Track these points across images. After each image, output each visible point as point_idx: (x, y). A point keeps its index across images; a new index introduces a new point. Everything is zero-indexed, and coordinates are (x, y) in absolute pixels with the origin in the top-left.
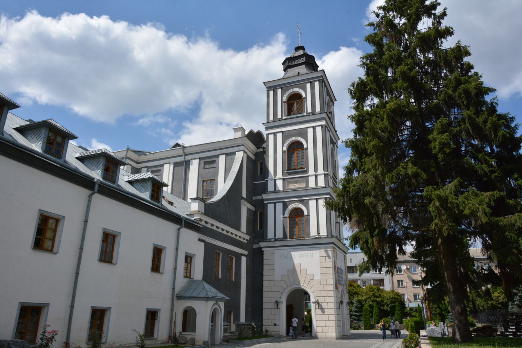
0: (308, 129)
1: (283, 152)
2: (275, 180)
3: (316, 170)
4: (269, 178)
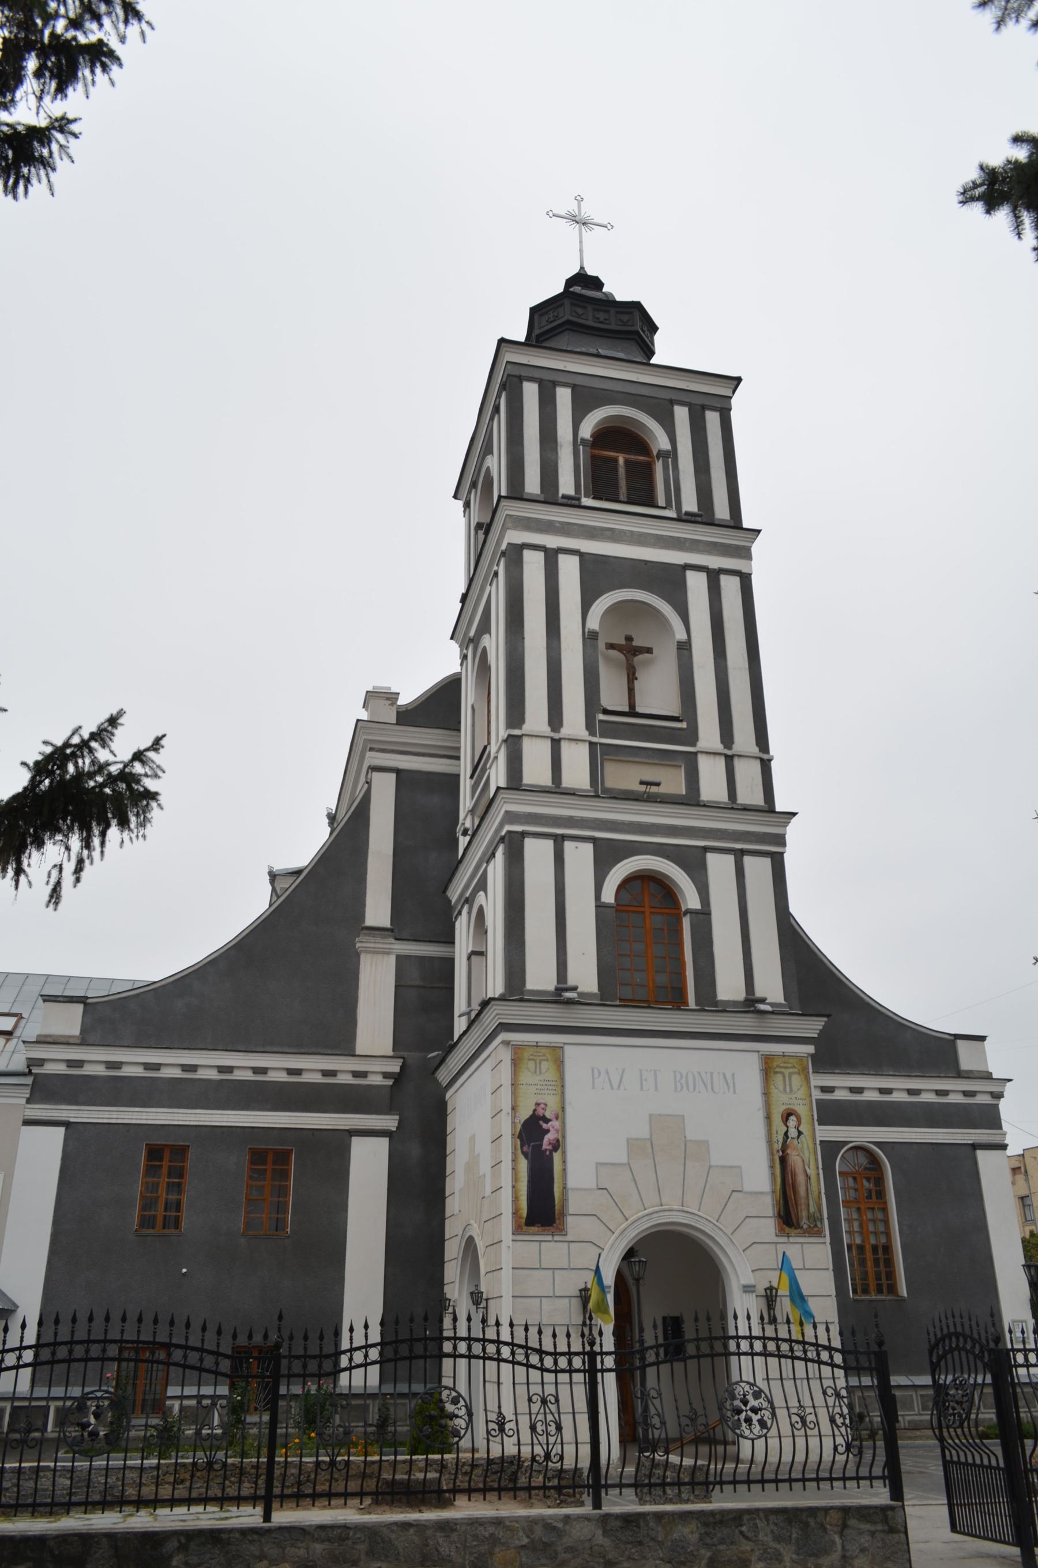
0: (690, 575)
1: (590, 638)
2: (556, 744)
4: (525, 727)
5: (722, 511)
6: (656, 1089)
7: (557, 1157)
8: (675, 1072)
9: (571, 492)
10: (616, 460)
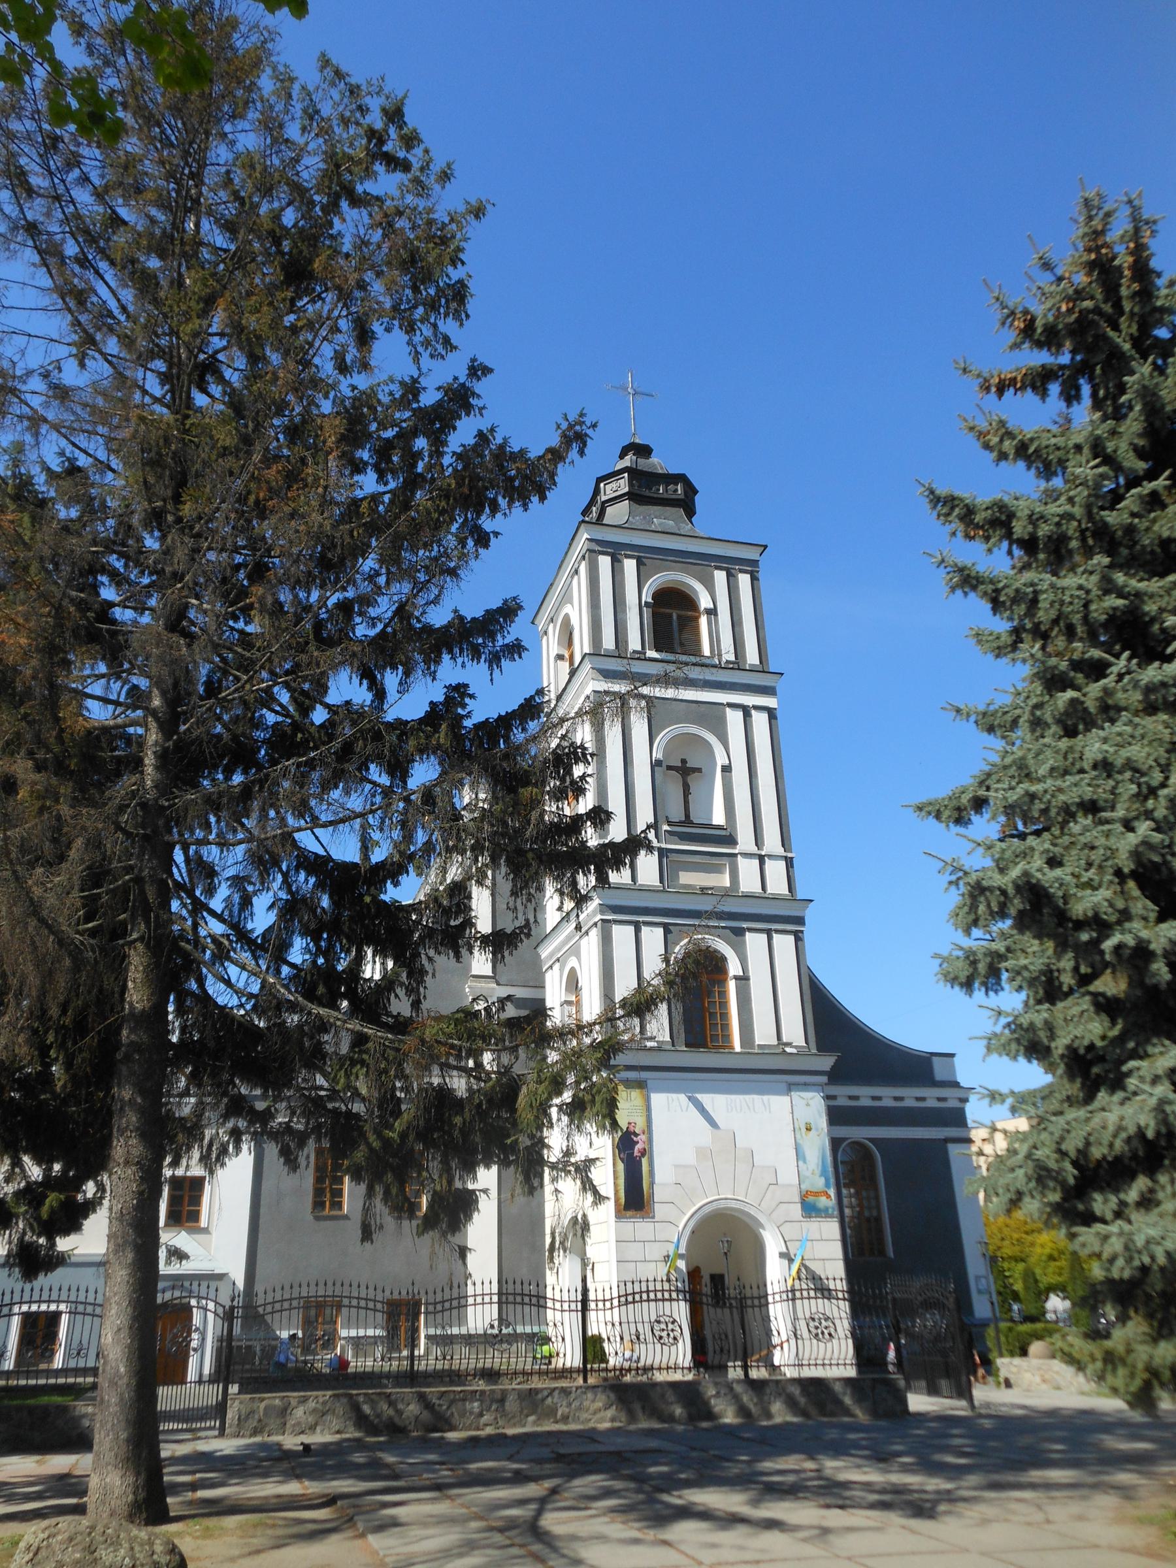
1: (655, 765)
3: (758, 840)
5: (752, 657)
7: (644, 1161)
9: (639, 648)
10: (671, 616)
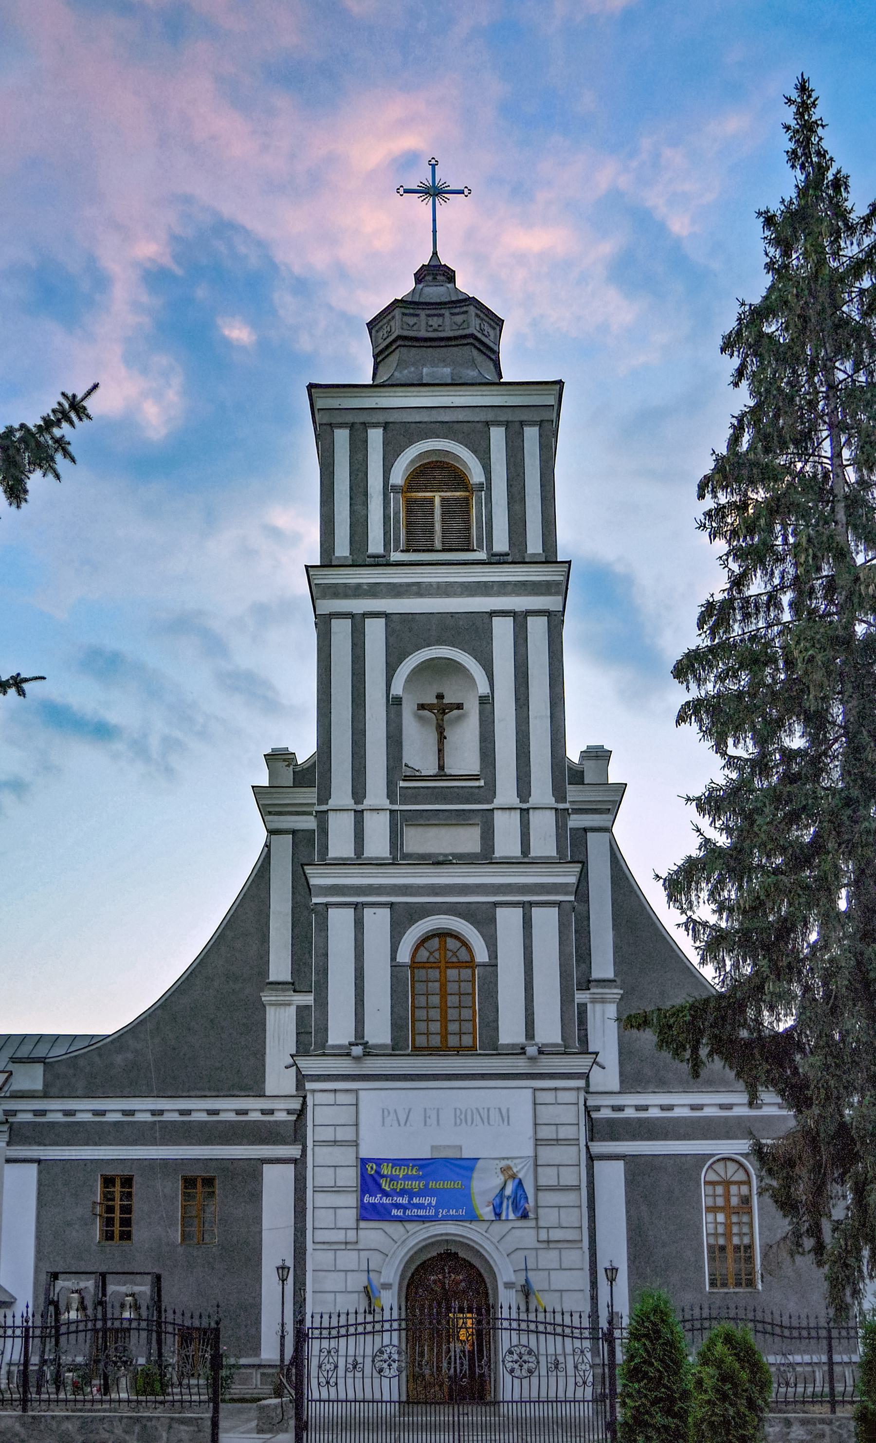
1: (394, 703)
2: (359, 815)
5: (534, 546)
6: (438, 1124)
8: (455, 1109)
9: (380, 550)
10: (431, 501)
